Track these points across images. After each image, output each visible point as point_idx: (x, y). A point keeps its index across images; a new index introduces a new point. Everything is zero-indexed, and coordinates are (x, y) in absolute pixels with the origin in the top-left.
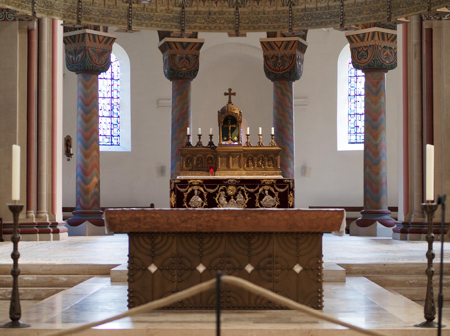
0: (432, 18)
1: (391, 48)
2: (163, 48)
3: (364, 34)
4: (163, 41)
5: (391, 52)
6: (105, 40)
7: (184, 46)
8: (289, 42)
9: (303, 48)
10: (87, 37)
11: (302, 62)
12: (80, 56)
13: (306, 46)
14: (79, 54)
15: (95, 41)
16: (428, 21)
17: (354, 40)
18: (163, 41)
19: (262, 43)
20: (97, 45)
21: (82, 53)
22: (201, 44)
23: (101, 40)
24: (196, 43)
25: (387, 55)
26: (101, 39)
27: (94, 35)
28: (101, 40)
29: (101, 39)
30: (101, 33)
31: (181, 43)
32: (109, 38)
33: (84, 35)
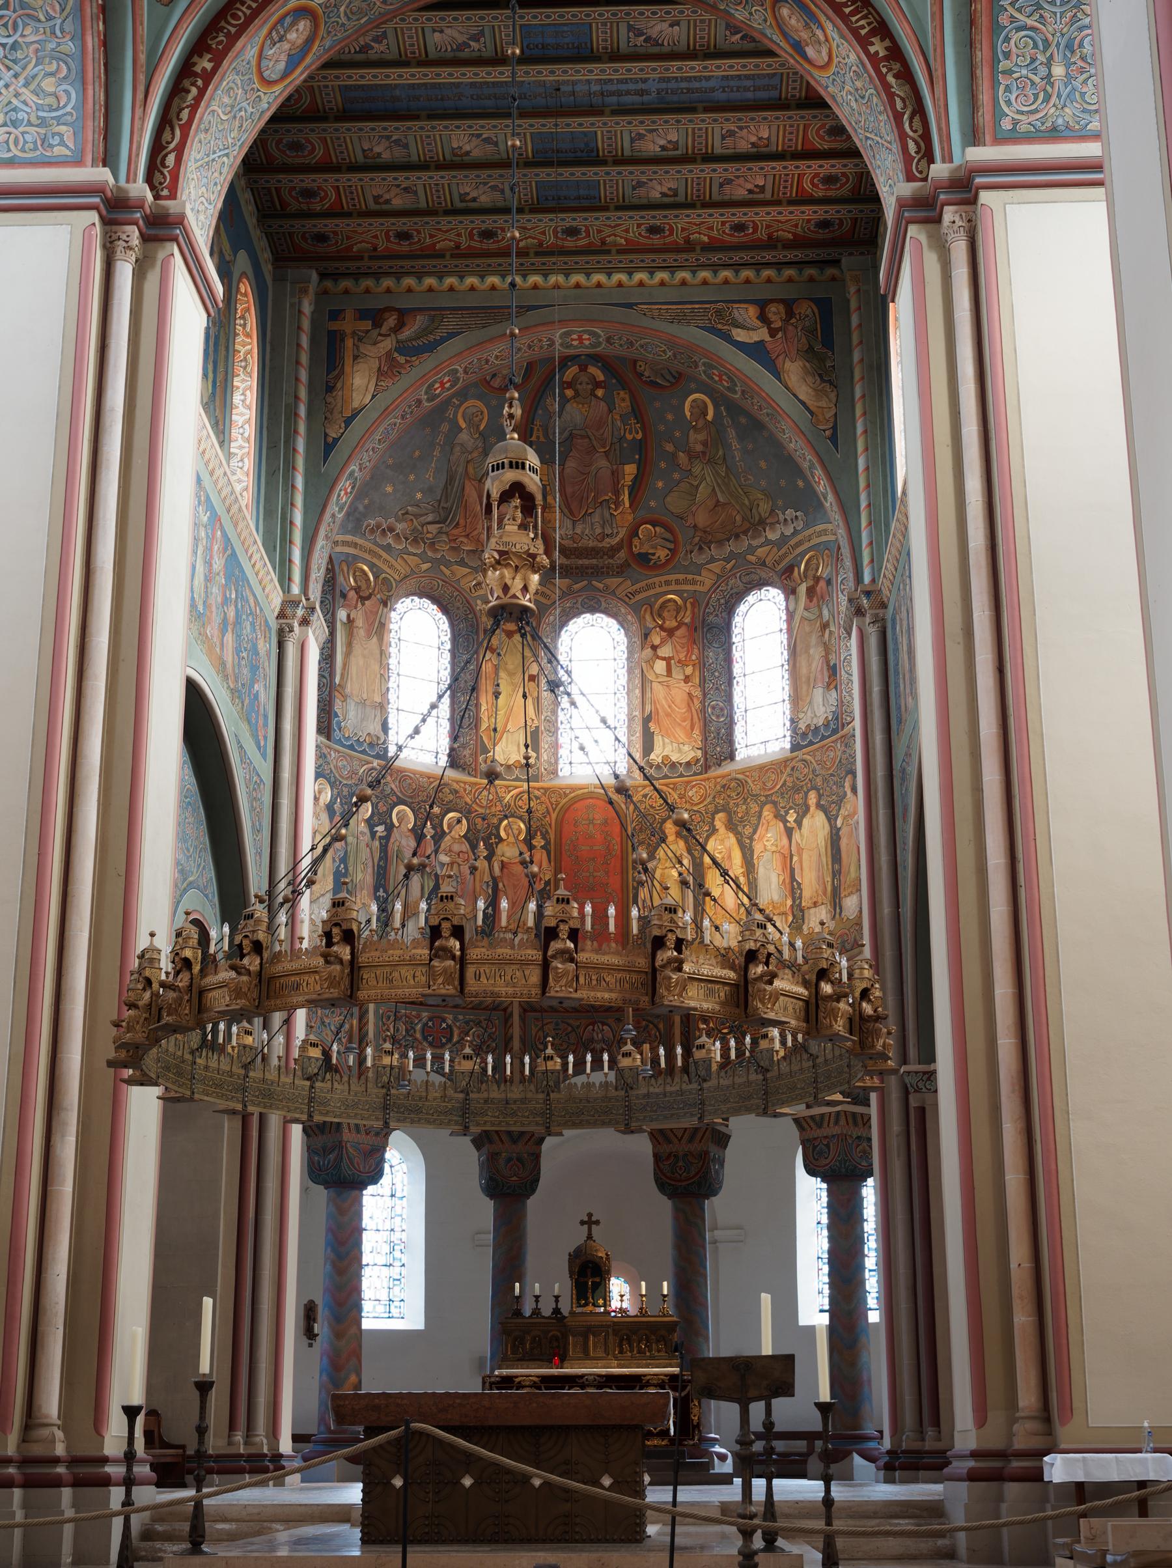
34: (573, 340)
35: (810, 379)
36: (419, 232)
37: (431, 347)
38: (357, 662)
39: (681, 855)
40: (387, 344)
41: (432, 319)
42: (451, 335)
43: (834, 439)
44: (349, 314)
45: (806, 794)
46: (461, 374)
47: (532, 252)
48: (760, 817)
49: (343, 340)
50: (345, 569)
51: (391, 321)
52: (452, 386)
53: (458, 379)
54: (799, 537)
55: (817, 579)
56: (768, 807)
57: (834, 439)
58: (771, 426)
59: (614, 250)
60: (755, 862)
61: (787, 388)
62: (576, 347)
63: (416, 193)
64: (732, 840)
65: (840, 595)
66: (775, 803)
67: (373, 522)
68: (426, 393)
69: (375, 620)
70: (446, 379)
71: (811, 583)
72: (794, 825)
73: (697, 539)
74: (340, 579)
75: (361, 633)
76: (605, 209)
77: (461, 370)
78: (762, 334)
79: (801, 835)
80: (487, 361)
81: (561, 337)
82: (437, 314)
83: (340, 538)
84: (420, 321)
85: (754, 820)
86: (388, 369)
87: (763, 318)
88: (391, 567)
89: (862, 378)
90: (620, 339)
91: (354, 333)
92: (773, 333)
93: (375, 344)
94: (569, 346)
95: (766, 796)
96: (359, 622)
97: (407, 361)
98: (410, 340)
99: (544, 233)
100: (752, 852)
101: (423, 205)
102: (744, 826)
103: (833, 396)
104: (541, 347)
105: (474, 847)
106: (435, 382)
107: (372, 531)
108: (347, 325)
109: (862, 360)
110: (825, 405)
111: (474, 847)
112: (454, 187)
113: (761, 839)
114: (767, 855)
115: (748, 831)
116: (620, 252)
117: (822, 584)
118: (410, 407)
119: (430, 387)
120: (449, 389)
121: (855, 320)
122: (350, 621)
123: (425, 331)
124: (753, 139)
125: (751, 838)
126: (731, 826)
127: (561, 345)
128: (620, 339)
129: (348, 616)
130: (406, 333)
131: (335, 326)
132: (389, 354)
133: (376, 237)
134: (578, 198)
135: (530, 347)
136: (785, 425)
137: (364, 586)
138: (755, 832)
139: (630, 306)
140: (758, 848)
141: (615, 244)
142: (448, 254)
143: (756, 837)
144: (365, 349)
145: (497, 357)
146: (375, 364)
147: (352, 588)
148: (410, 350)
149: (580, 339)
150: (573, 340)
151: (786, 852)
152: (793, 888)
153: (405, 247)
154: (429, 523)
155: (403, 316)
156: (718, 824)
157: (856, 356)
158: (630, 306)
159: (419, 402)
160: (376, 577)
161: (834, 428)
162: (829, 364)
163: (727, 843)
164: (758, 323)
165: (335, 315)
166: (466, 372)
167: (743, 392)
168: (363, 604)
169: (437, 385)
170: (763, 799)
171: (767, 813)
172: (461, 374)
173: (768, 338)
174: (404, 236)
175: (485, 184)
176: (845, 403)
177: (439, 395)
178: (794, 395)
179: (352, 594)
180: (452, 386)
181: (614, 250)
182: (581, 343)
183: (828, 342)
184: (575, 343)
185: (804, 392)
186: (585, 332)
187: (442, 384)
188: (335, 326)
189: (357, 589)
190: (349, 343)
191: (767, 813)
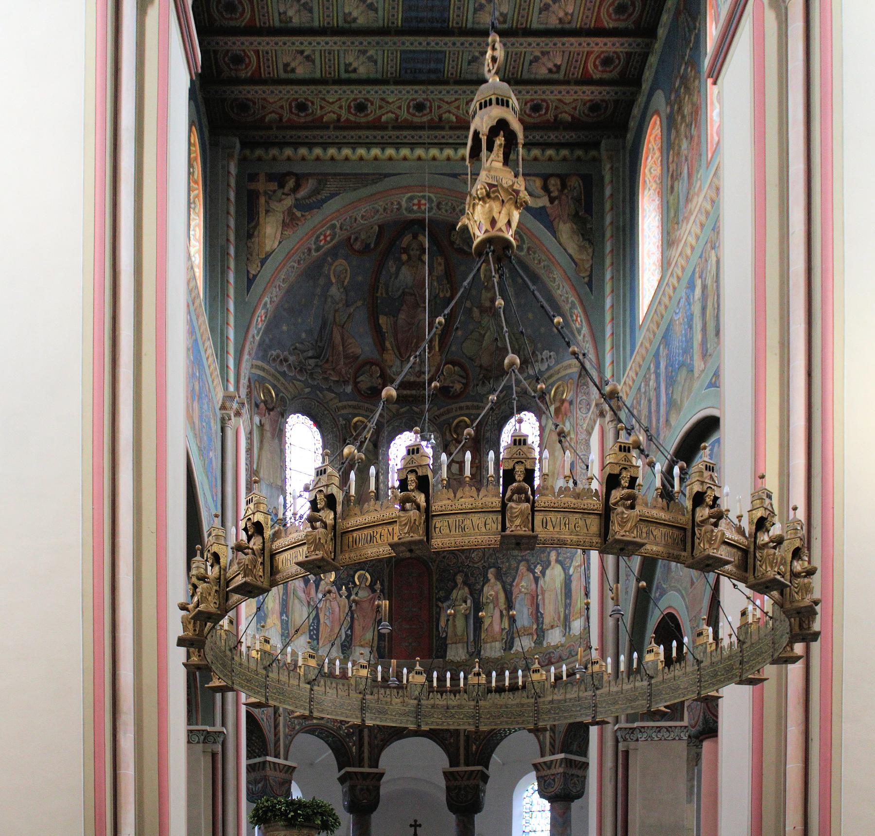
0: (629, 740)
1: (578, 776)
2: (342, 780)
3: (552, 761)
4: (343, 772)
5: (578, 781)
6: (286, 768)
7: (365, 776)
8: (472, 771)
9: (485, 778)
10: (268, 765)
11: (484, 795)
12: (260, 785)
13: (488, 777)
14: (259, 783)
15: (275, 770)
16: (625, 743)
17: (540, 767)
18: (343, 772)
19: (444, 773)
20: (278, 774)
21: (262, 783)
22: (382, 775)
23: (281, 768)
24: (377, 773)
25: (575, 783)
26: (281, 767)
27: (274, 763)
28: (281, 768)
29: (281, 767)
30: (281, 761)
31: (362, 773)
32: (290, 767)
33: (265, 762)
34: (414, 205)
35: (576, 238)
36: (313, 103)
37: (320, 204)
38: (266, 455)
39: (466, 597)
40: (289, 202)
41: (319, 182)
42: (332, 196)
43: (590, 284)
44: (262, 178)
45: (549, 553)
46: (338, 230)
47: (390, 126)
48: (517, 570)
49: (258, 198)
50: (258, 386)
51: (291, 183)
52: (332, 240)
53: (336, 234)
54: (551, 371)
55: (563, 401)
56: (523, 563)
57: (590, 284)
58: (545, 278)
59: (447, 127)
60: (514, 600)
61: (560, 244)
62: (415, 212)
63: (313, 61)
64: (499, 586)
65: (579, 412)
66: (527, 561)
67: (274, 353)
68: (315, 243)
69: (276, 426)
70: (328, 233)
71: (558, 404)
72: (541, 575)
73: (481, 376)
74: (255, 393)
75: (268, 435)
76: (446, 83)
77: (338, 226)
78: (544, 202)
79: (545, 582)
80: (356, 219)
81: (406, 202)
82: (322, 179)
83: (256, 362)
84: (309, 186)
85: (513, 572)
86: (290, 222)
87: (545, 188)
88: (286, 388)
89: (612, 236)
90: (447, 204)
91: (265, 193)
92: (552, 201)
93: (280, 200)
94: (410, 210)
95: (522, 556)
96: (267, 427)
97: (303, 216)
98: (304, 198)
99: (400, 107)
100: (512, 594)
101: (318, 75)
102: (507, 577)
103: (590, 250)
104: (392, 211)
105: (339, 589)
106: (321, 234)
107: (274, 360)
108: (261, 185)
109: (612, 223)
110: (584, 257)
111: (339, 589)
112: (342, 55)
113: (517, 585)
114: (521, 596)
115: (509, 580)
116: (452, 128)
117: (566, 404)
118: (304, 253)
119: (318, 237)
120: (329, 243)
121: (608, 192)
122: (262, 425)
123: (316, 192)
124: (561, 14)
125: (511, 585)
126: (499, 577)
127: (406, 209)
128: (447, 204)
129: (260, 421)
130: (302, 193)
131: (253, 186)
132: (290, 210)
133: (282, 107)
134: (430, 71)
135: (385, 209)
136: (557, 274)
137: (269, 401)
138: (513, 581)
139: (455, 176)
140: (515, 591)
141: (449, 122)
142: (332, 126)
143: (514, 584)
144: (274, 205)
145: (363, 216)
146: (280, 216)
147: (262, 401)
148: (306, 206)
149: (419, 204)
150: (414, 205)
151: (534, 594)
152: (537, 617)
153: (302, 118)
154: (311, 358)
155: (300, 180)
156: (490, 576)
157: (608, 219)
158: (455, 176)
159: (310, 250)
160: (277, 395)
161: (590, 276)
162: (589, 226)
163: (495, 588)
164: (542, 193)
165: (253, 178)
166: (341, 228)
167: (529, 249)
168: (269, 414)
169: (322, 237)
170: (520, 558)
171: (522, 568)
172: (338, 230)
173: (548, 204)
174: (302, 107)
175: (364, 52)
176: (598, 257)
177: (323, 246)
178: (565, 250)
179: (262, 406)
180: (332, 240)
181: (447, 127)
182: (419, 207)
183: (589, 210)
184: (415, 208)
185: (572, 248)
186: (424, 197)
187: (325, 237)
188: (253, 186)
189: (265, 402)
190: (262, 200)
191: (522, 568)
